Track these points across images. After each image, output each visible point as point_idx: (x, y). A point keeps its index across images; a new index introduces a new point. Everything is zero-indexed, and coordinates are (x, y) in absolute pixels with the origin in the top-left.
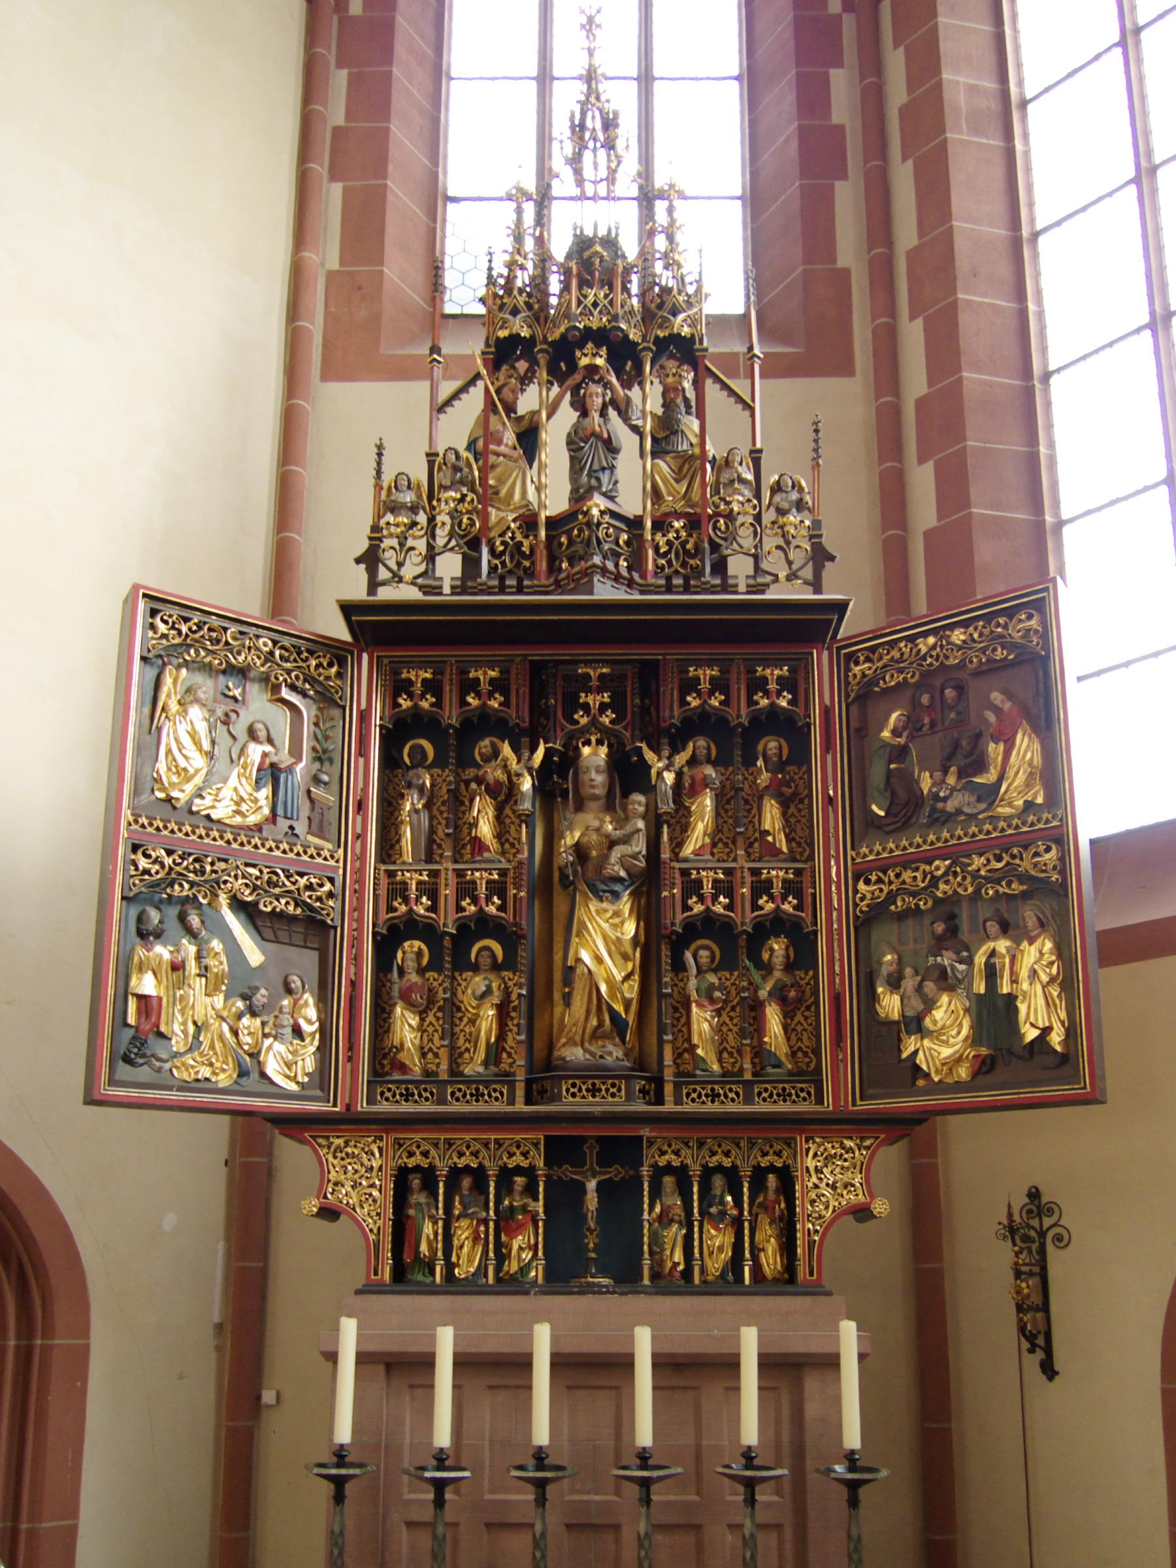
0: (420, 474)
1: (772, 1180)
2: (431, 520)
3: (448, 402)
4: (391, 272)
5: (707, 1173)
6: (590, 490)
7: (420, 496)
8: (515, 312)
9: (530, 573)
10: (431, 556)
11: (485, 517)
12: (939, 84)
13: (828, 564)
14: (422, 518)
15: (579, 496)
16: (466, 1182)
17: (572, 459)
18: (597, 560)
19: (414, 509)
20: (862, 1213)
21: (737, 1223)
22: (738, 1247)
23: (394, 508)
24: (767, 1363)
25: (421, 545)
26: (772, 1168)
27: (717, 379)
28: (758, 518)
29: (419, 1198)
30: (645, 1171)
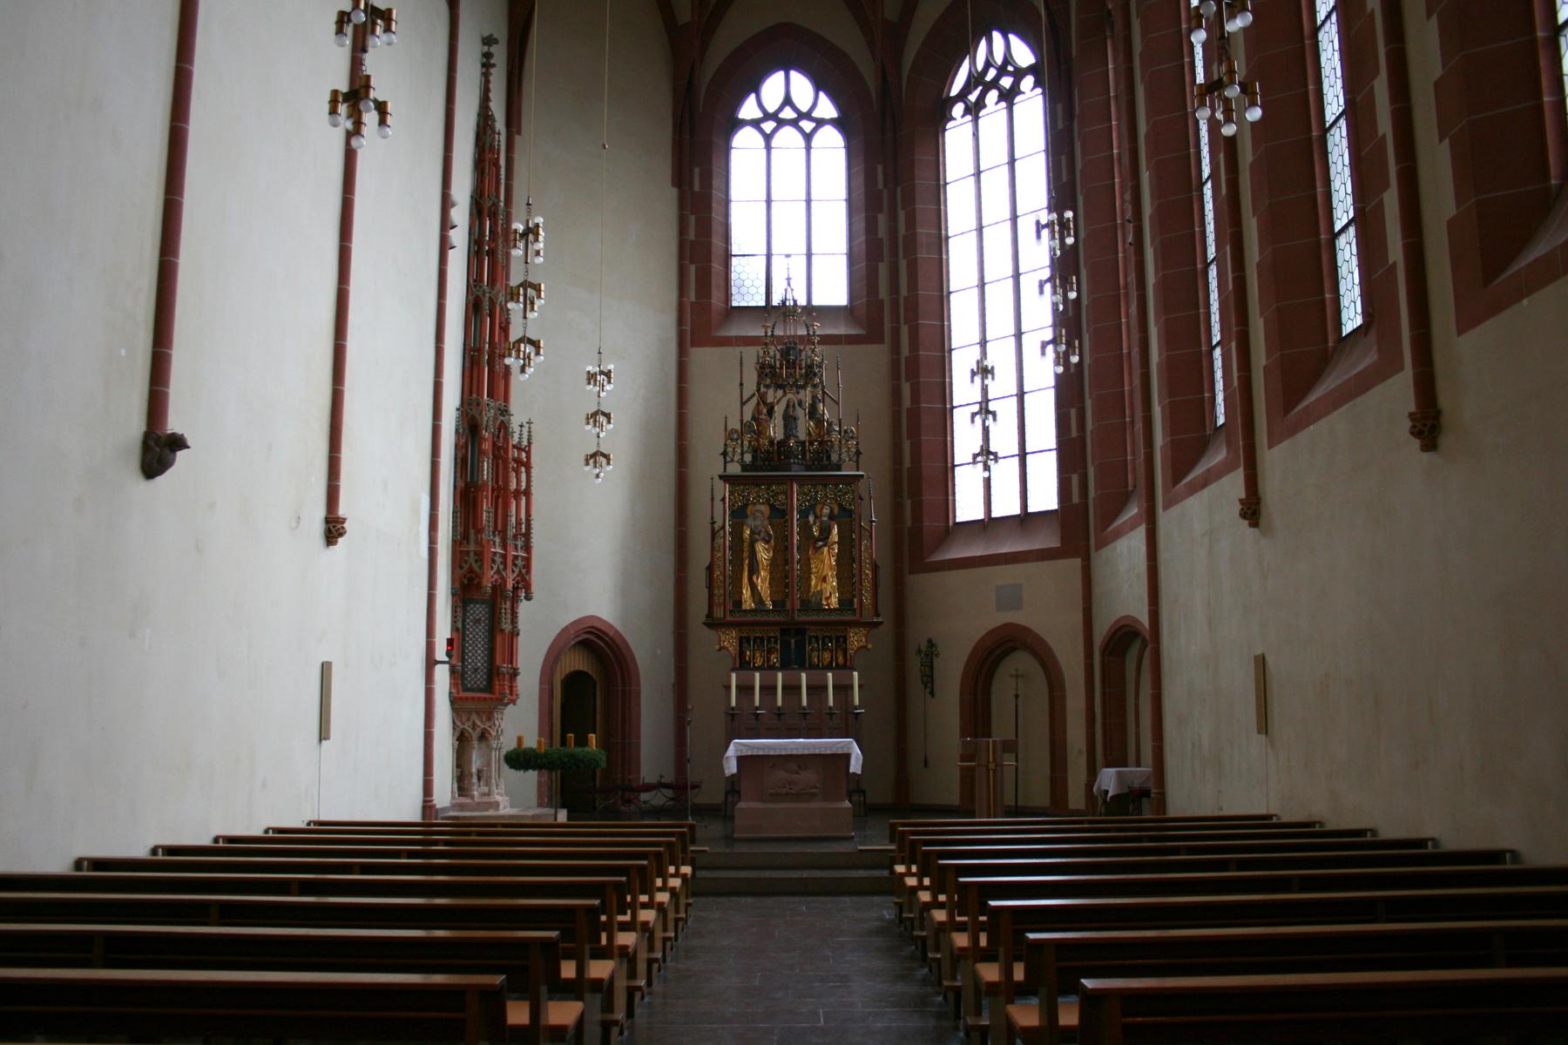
0: (738, 427)
1: (841, 640)
2: (742, 442)
3: (746, 402)
4: (714, 301)
6: (790, 435)
7: (738, 435)
8: (766, 375)
9: (772, 459)
10: (742, 454)
11: (758, 442)
12: (915, 233)
13: (861, 456)
14: (739, 442)
16: (758, 640)
17: (785, 424)
18: (792, 461)
20: (864, 647)
22: (832, 658)
23: (732, 440)
25: (739, 451)
26: (841, 636)
27: (828, 395)
28: (840, 442)
29: (745, 645)
30: (807, 637)
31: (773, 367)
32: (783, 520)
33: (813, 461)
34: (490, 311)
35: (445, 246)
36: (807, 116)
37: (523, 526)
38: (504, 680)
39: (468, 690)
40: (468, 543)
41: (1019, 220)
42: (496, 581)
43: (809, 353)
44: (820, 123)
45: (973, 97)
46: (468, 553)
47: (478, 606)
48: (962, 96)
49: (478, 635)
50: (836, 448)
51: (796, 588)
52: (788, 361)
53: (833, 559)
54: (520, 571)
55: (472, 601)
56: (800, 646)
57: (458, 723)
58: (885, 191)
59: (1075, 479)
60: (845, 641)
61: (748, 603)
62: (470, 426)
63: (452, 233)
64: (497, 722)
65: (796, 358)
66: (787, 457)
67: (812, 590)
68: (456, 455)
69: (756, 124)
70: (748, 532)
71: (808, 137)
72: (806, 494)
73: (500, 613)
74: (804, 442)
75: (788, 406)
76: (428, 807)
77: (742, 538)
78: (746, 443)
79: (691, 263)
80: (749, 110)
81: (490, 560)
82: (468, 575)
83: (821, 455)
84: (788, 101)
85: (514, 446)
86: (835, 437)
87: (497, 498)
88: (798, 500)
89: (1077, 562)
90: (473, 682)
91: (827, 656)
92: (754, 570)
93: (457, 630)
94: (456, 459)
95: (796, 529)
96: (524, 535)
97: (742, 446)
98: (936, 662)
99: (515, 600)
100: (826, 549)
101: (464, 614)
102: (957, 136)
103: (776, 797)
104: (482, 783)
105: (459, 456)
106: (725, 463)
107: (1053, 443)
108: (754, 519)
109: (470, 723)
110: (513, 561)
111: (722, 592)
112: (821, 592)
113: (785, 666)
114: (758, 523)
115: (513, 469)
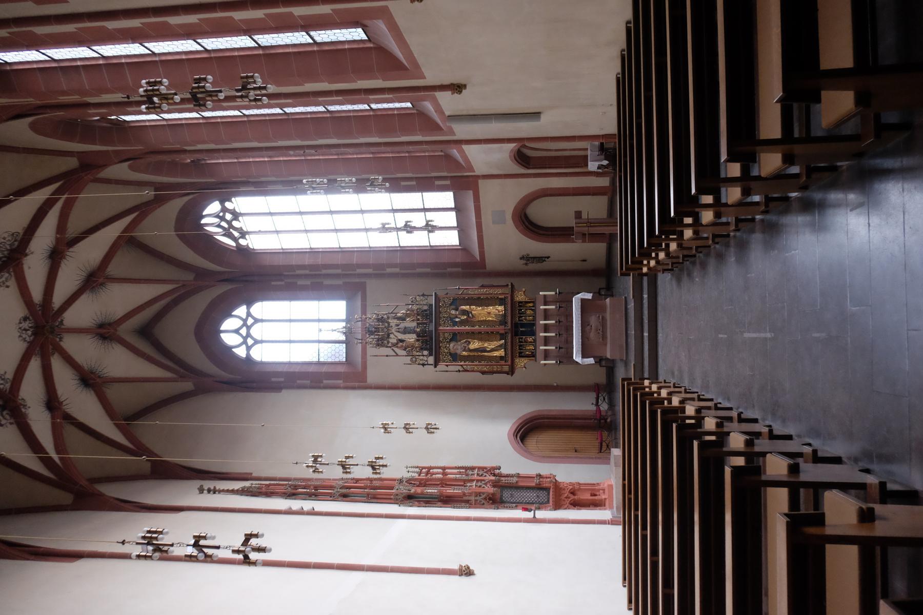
2: (417, 356)
5: (519, 313)
9: (426, 340)
10: (423, 356)
12: (308, 265)
14: (417, 357)
15: (414, 332)
19: (416, 358)
21: (526, 309)
22: (530, 309)
23: (416, 361)
24: (545, 305)
25: (422, 357)
28: (417, 305)
31: (378, 340)
32: (458, 335)
33: (427, 319)
34: (347, 488)
35: (313, 513)
36: (245, 321)
37: (461, 471)
38: (542, 481)
39: (548, 501)
40: (471, 501)
41: (301, 211)
42: (491, 485)
43: (371, 320)
44: (249, 314)
45: (236, 234)
46: (476, 500)
47: (504, 495)
48: (235, 239)
49: (519, 495)
50: (421, 307)
51: (493, 328)
52: (375, 332)
53: (479, 309)
54: (485, 472)
55: (501, 498)
56: (523, 325)
57: (566, 506)
58: (286, 281)
59: (437, 183)
60: (521, 302)
61: (501, 353)
62: (409, 499)
63: (305, 509)
64: (566, 485)
65: (374, 327)
66: (425, 332)
67: (494, 319)
68: (423, 507)
69: (249, 348)
70: (464, 353)
71: (257, 321)
72: (445, 323)
73: (507, 483)
74: (417, 323)
75: (399, 332)
76: (612, 522)
77: (467, 356)
78: (417, 354)
79: (322, 382)
80: (241, 352)
81: (480, 488)
82: (488, 500)
83: (424, 314)
84: (237, 331)
85: (419, 475)
86: (415, 307)
87: (446, 485)
88: (447, 327)
89: (480, 182)
90: (544, 498)
91: (529, 312)
92: (484, 350)
93: (516, 506)
94: (426, 507)
95: (463, 328)
96: (466, 470)
97: (419, 356)
98: (531, 255)
99: (500, 475)
100: (473, 312)
101: (509, 502)
102: (255, 243)
103: (604, 337)
104: (598, 494)
105: (424, 505)
106: (428, 364)
107: (418, 195)
108: (458, 349)
109: (566, 500)
110: (480, 476)
111: (495, 367)
112: (496, 315)
113: (533, 333)
114: (459, 347)
115: (431, 476)
